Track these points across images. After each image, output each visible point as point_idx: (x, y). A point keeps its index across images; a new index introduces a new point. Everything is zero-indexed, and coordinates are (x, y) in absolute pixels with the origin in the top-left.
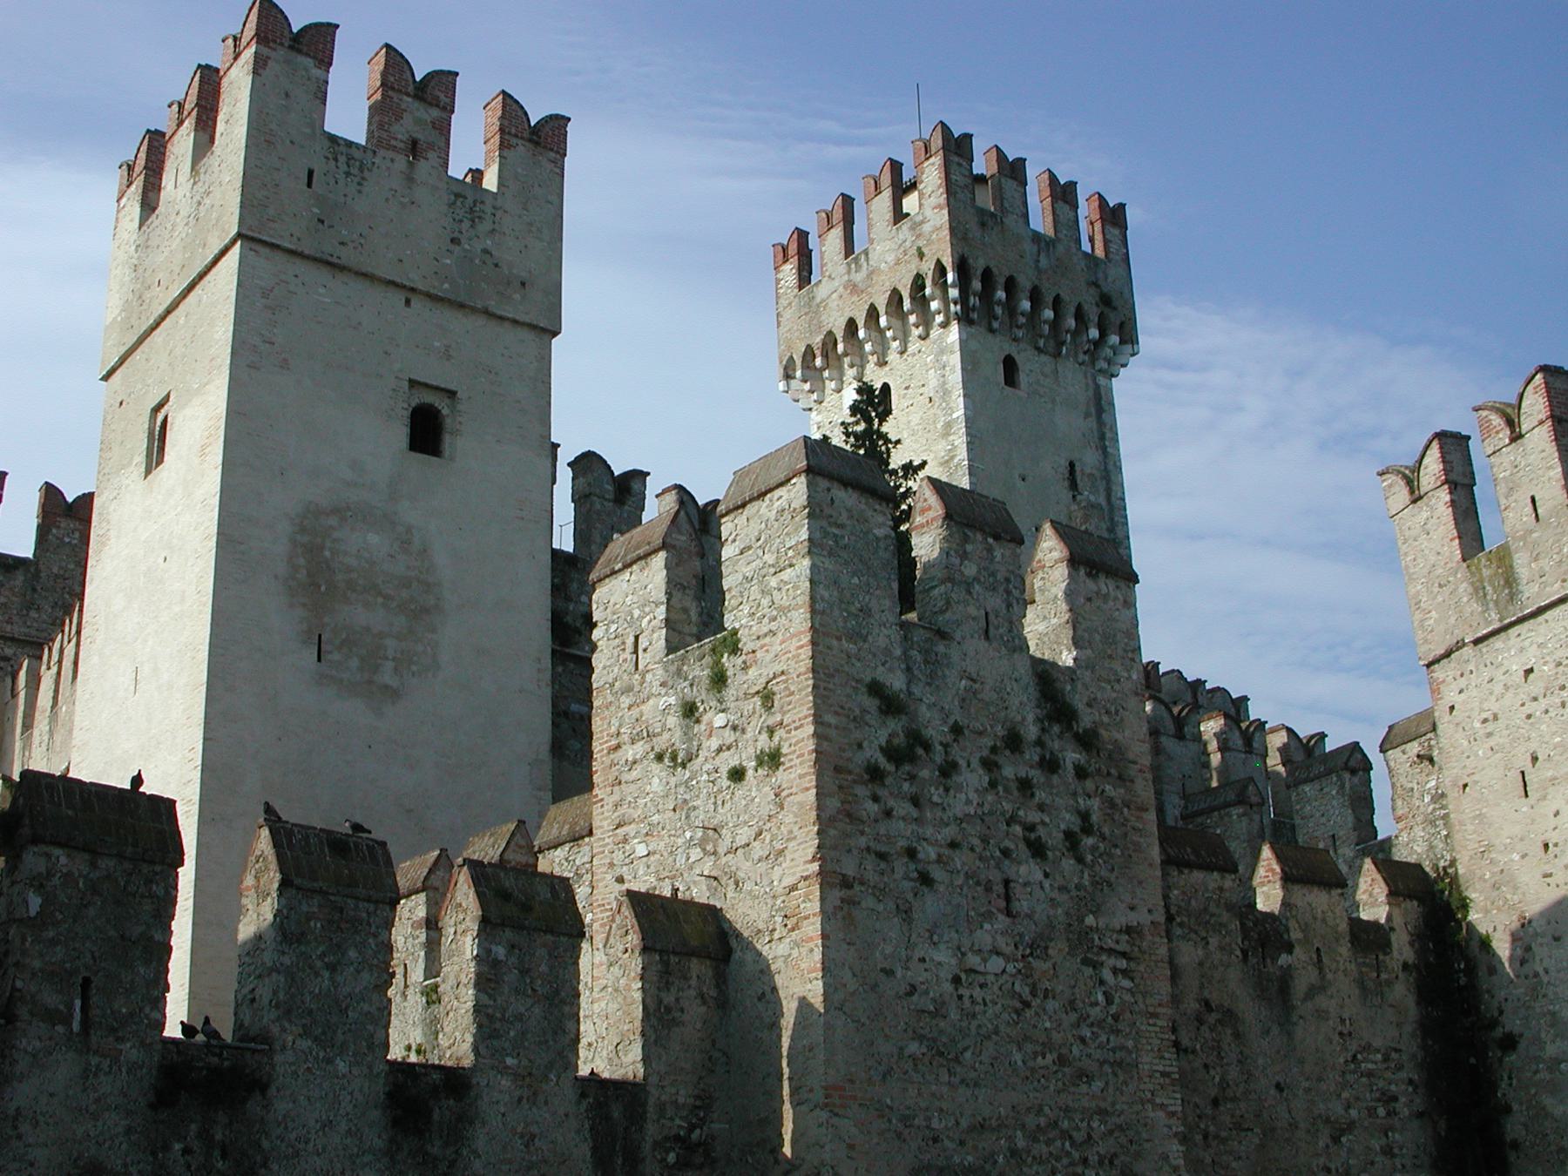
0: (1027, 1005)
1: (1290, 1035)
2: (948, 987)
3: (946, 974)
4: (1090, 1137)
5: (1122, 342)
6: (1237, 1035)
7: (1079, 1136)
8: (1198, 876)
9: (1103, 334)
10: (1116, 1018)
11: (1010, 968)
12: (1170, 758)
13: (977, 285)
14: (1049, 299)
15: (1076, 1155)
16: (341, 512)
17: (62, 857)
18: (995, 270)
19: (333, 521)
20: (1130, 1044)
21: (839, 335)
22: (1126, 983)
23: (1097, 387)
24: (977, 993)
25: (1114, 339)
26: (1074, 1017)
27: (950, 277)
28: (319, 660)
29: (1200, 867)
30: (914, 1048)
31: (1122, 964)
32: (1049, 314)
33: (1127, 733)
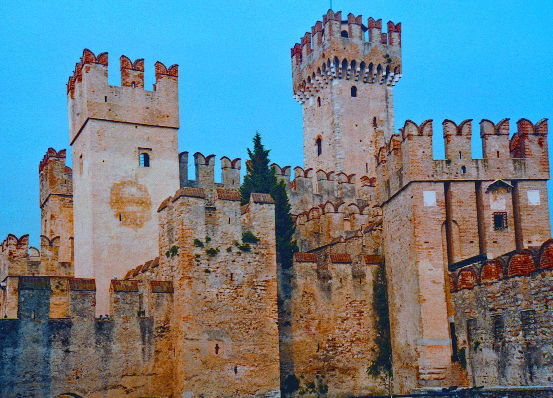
0: (236, 298)
1: (330, 299)
2: (215, 296)
3: (215, 294)
4: (251, 324)
5: (395, 74)
6: (314, 299)
7: (248, 324)
8: (306, 263)
9: (388, 72)
10: (260, 300)
11: (232, 291)
12: (357, 220)
13: (340, 66)
14: (367, 65)
15: (247, 327)
16: (123, 184)
17: (27, 291)
18: (348, 59)
19: (121, 187)
20: (264, 305)
21: (306, 81)
22: (264, 292)
23: (387, 91)
24: (222, 297)
25: (392, 74)
26: (248, 300)
27: (332, 65)
28: (120, 220)
29: (305, 262)
30: (205, 308)
31: (263, 288)
32: (367, 70)
33: (269, 238)
